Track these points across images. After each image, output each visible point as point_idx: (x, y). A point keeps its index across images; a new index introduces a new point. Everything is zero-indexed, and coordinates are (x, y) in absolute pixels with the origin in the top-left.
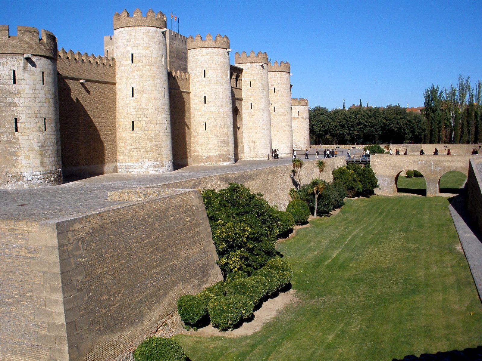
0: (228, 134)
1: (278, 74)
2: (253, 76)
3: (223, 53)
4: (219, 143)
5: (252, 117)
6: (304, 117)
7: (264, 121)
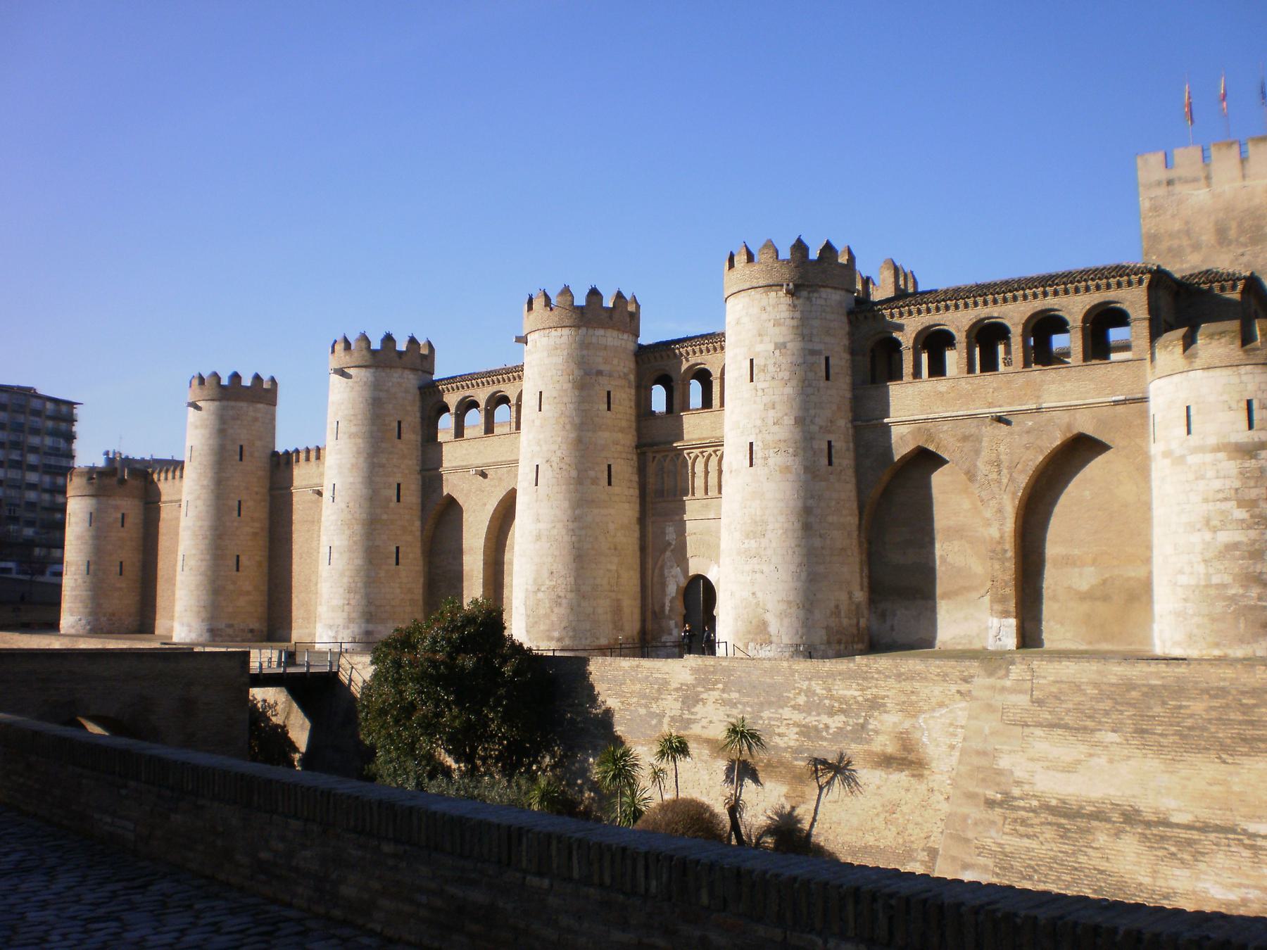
6: (1174, 445)
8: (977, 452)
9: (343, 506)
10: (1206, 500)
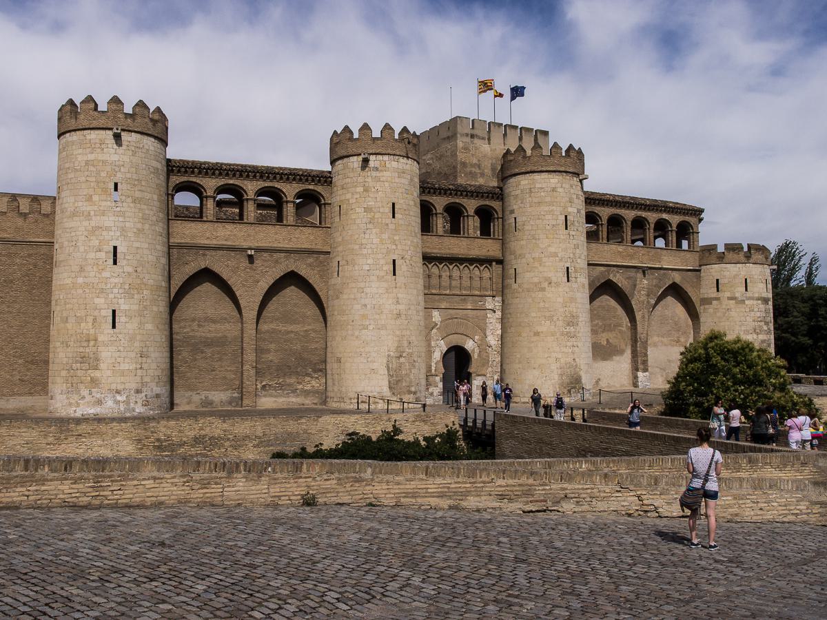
0: (96, 340)
1: (524, 181)
2: (344, 191)
3: (97, 141)
4: (71, 361)
5: (338, 298)
7: (365, 305)
8: (635, 286)
9: (130, 269)
10: (754, 321)
